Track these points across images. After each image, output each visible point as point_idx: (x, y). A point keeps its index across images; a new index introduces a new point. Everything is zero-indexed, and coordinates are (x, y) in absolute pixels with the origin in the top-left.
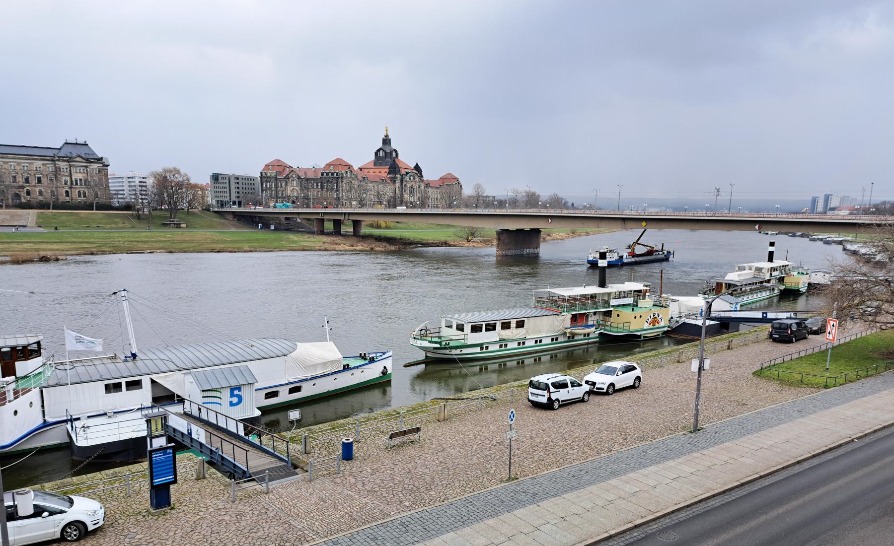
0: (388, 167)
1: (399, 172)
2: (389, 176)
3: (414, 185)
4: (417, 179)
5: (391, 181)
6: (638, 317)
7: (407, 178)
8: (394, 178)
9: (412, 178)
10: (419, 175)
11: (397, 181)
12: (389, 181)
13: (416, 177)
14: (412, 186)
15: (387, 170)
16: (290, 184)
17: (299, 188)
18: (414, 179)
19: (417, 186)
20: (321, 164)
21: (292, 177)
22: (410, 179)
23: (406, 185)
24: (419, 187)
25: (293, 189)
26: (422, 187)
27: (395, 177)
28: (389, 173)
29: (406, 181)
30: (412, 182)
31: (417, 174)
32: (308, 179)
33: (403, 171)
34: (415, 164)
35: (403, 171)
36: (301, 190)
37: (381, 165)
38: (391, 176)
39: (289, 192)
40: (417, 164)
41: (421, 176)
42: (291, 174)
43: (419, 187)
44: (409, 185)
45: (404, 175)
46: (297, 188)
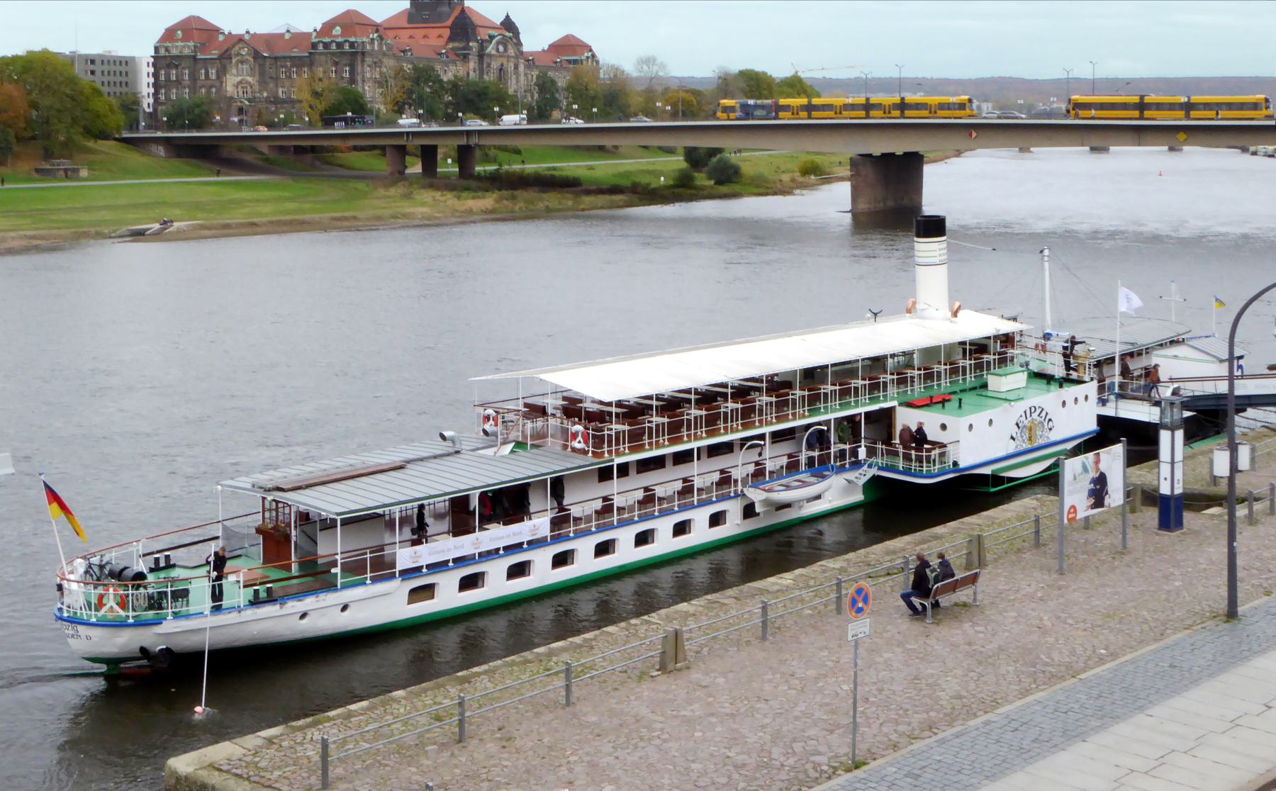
0: (449, 23)
1: (475, 35)
2: (450, 45)
3: (505, 63)
4: (511, 51)
5: (457, 55)
6: (1081, 399)
7: (490, 49)
8: (464, 48)
9: (501, 48)
10: (514, 40)
11: (470, 57)
12: (452, 57)
13: (510, 47)
14: (502, 65)
15: (447, 33)
16: (234, 71)
17: (257, 78)
18: (506, 50)
19: (512, 65)
20: (308, 20)
21: (238, 54)
22: (498, 50)
23: (489, 65)
24: (516, 67)
25: (240, 82)
26: (521, 68)
27: (467, 48)
28: (451, 39)
29: (490, 56)
30: (501, 56)
31: (510, 38)
32: (276, 58)
33: (483, 34)
34: (502, 18)
35: (483, 34)
36: (263, 83)
37: (425, 21)
38: (456, 44)
39: (228, 89)
40: (508, 17)
41: (519, 44)
42: (237, 48)
43: (516, 67)
44: (495, 65)
45: (486, 41)
46: (249, 79)
